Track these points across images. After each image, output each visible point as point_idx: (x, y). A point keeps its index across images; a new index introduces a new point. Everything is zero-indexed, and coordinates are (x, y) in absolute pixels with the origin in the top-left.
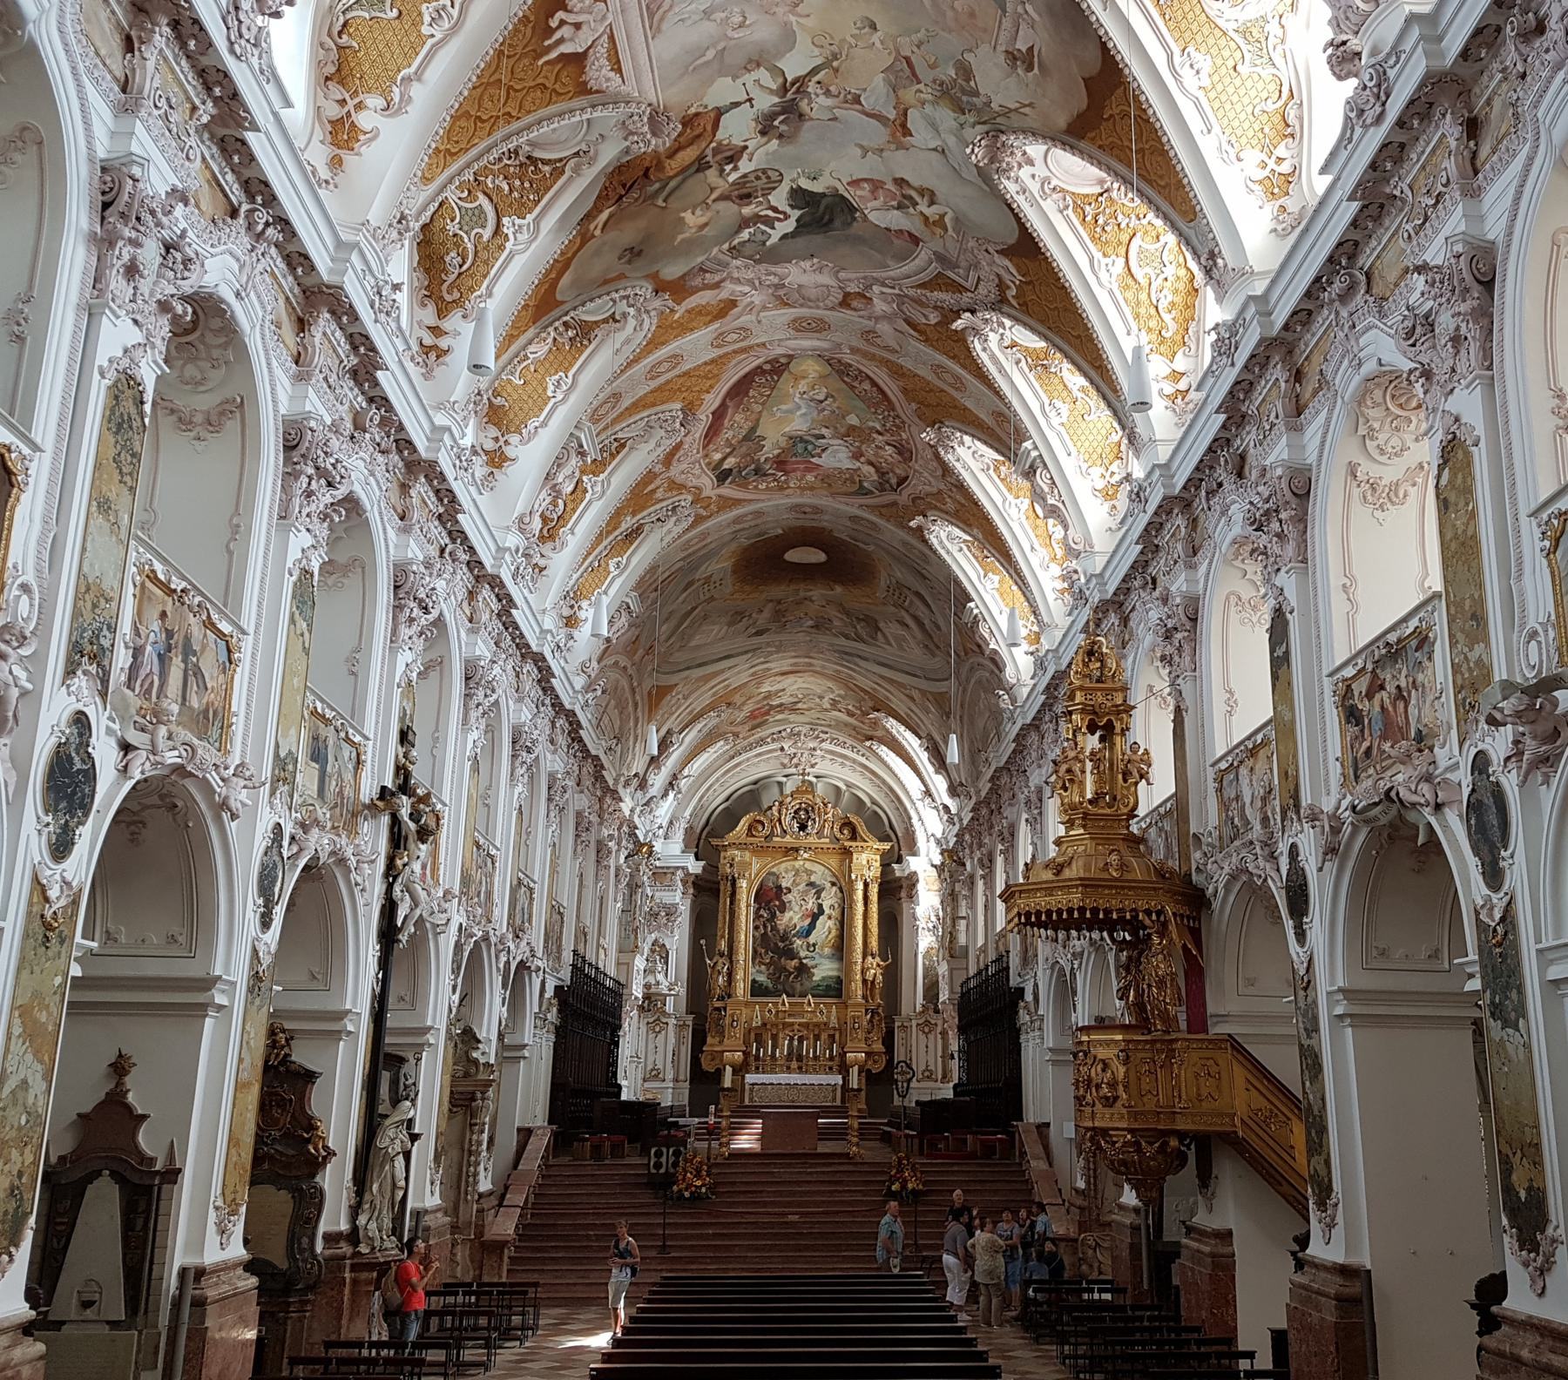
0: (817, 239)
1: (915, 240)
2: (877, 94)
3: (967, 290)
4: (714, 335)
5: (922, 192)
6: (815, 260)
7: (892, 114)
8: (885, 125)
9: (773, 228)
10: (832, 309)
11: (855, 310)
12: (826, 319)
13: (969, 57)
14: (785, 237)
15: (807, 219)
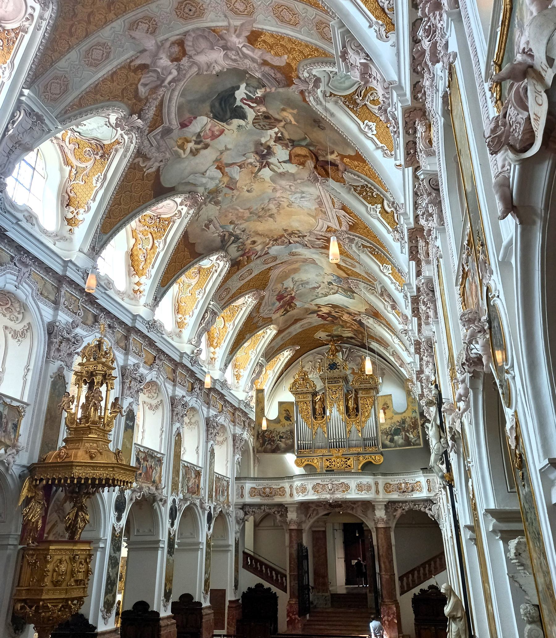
0: (220, 88)
1: (183, 125)
2: (235, 172)
3: (150, 132)
4: (254, 16)
5: (198, 150)
6: (214, 72)
7: (227, 169)
8: (226, 164)
9: (246, 94)
10: (186, 34)
11: (173, 43)
12: (181, 20)
13: (218, 208)
14: (238, 88)
15: (232, 100)
